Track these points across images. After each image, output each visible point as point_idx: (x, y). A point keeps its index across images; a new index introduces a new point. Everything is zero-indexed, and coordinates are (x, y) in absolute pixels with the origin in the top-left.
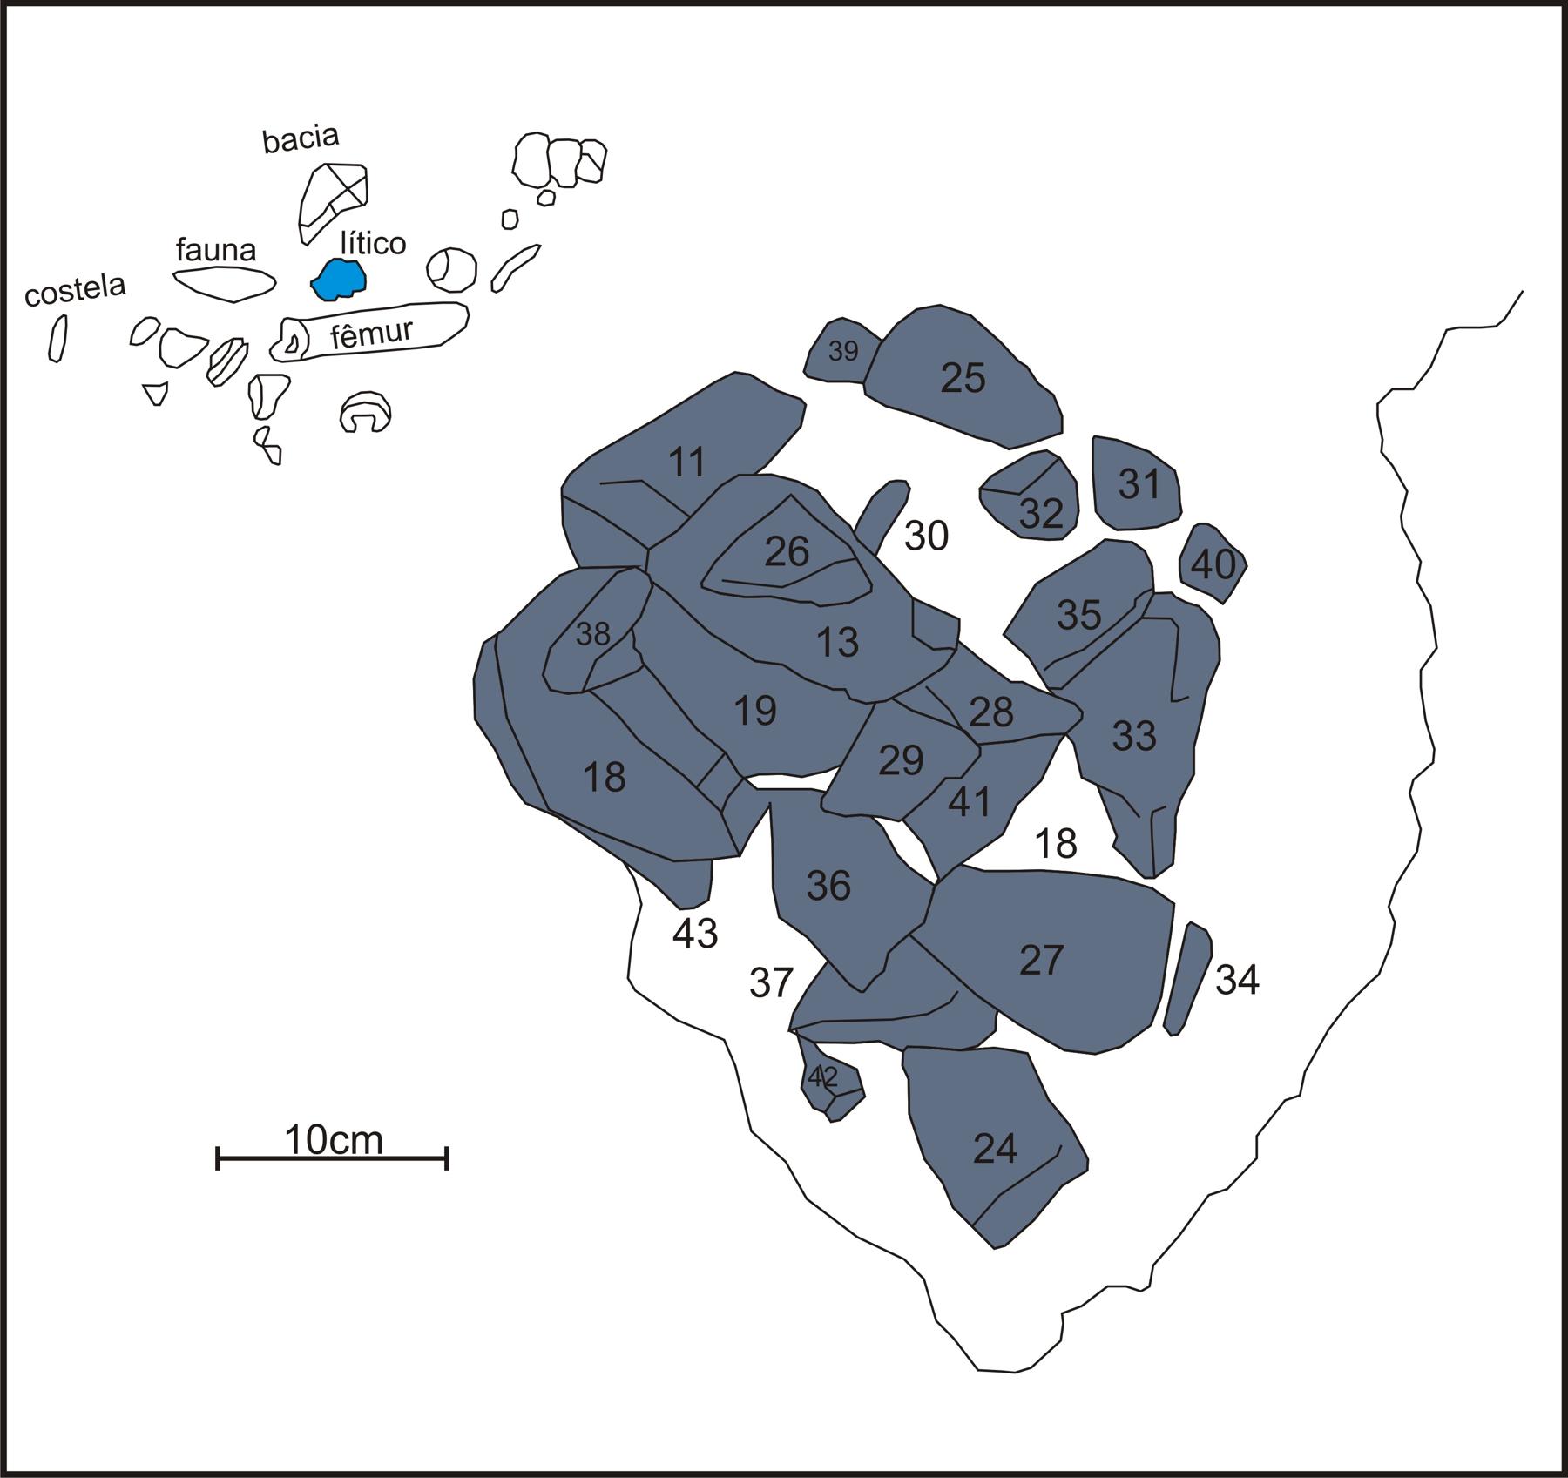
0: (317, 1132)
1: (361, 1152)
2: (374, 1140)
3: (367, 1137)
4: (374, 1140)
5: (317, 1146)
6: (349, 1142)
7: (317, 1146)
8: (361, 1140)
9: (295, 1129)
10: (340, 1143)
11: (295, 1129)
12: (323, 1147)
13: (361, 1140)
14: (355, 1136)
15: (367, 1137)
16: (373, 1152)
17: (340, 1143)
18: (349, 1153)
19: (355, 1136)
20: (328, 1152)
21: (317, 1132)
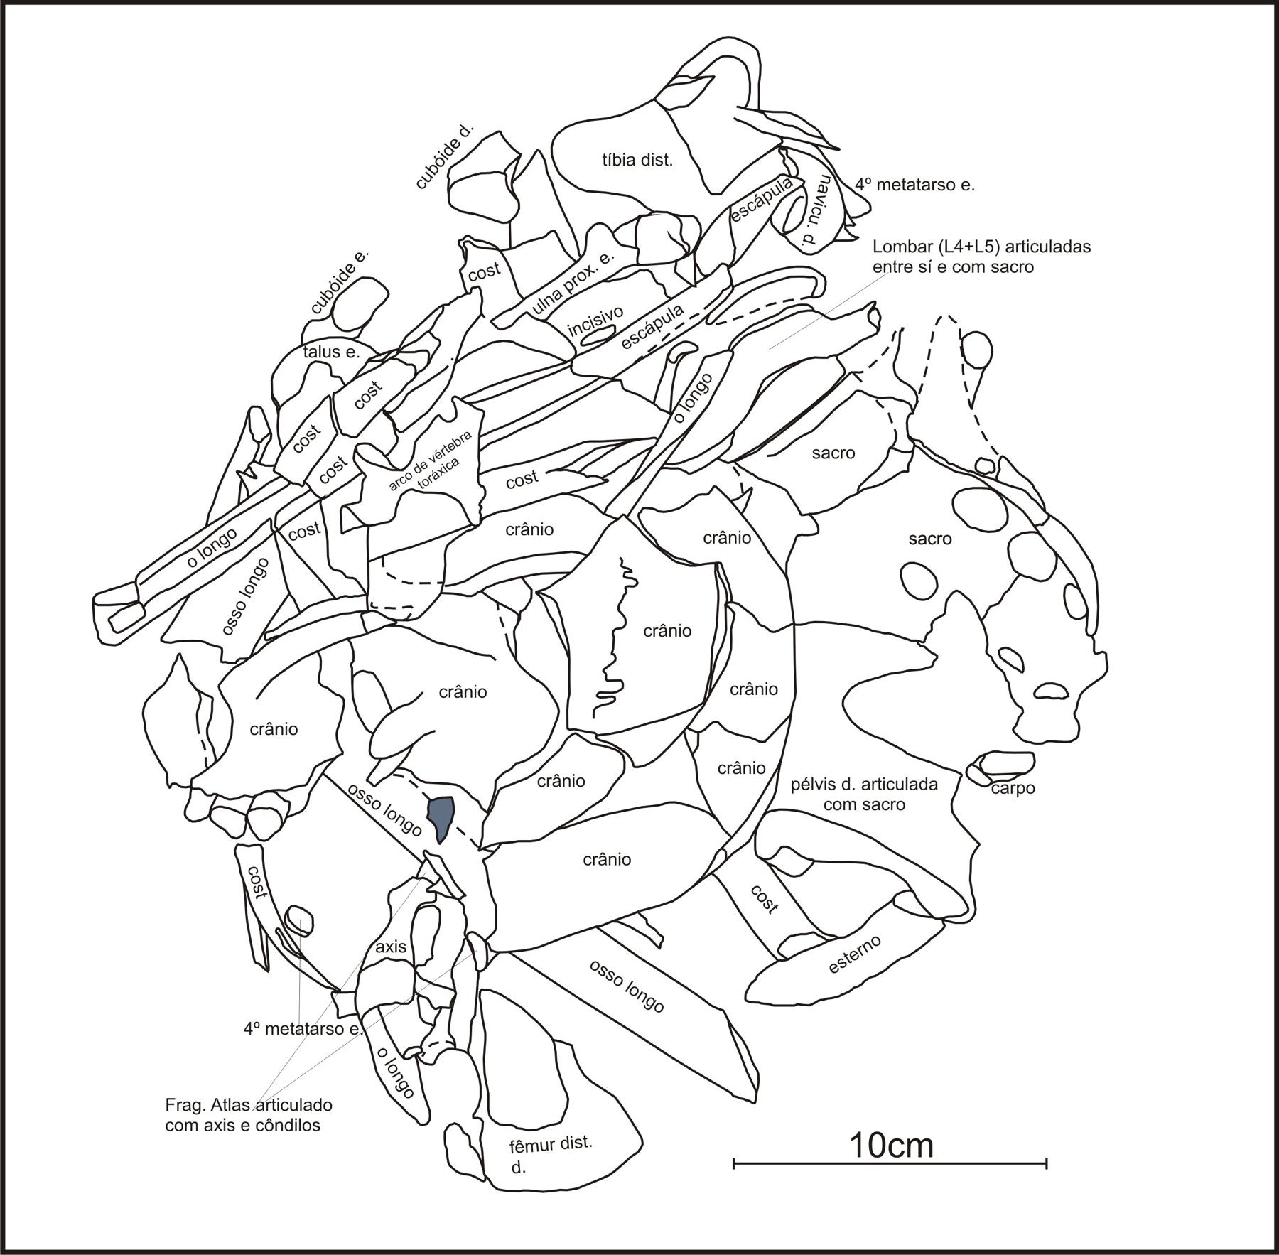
0: (877, 1139)
2: (925, 1145)
3: (920, 1143)
4: (925, 1145)
5: (877, 1151)
6: (905, 1148)
7: (877, 1151)
8: (915, 1145)
9: (858, 1136)
10: (897, 1148)
11: (858, 1136)
13: (915, 1145)
14: (909, 1142)
15: (920, 1143)
17: (897, 1148)
18: (904, 1159)
19: (909, 1142)
21: (877, 1139)
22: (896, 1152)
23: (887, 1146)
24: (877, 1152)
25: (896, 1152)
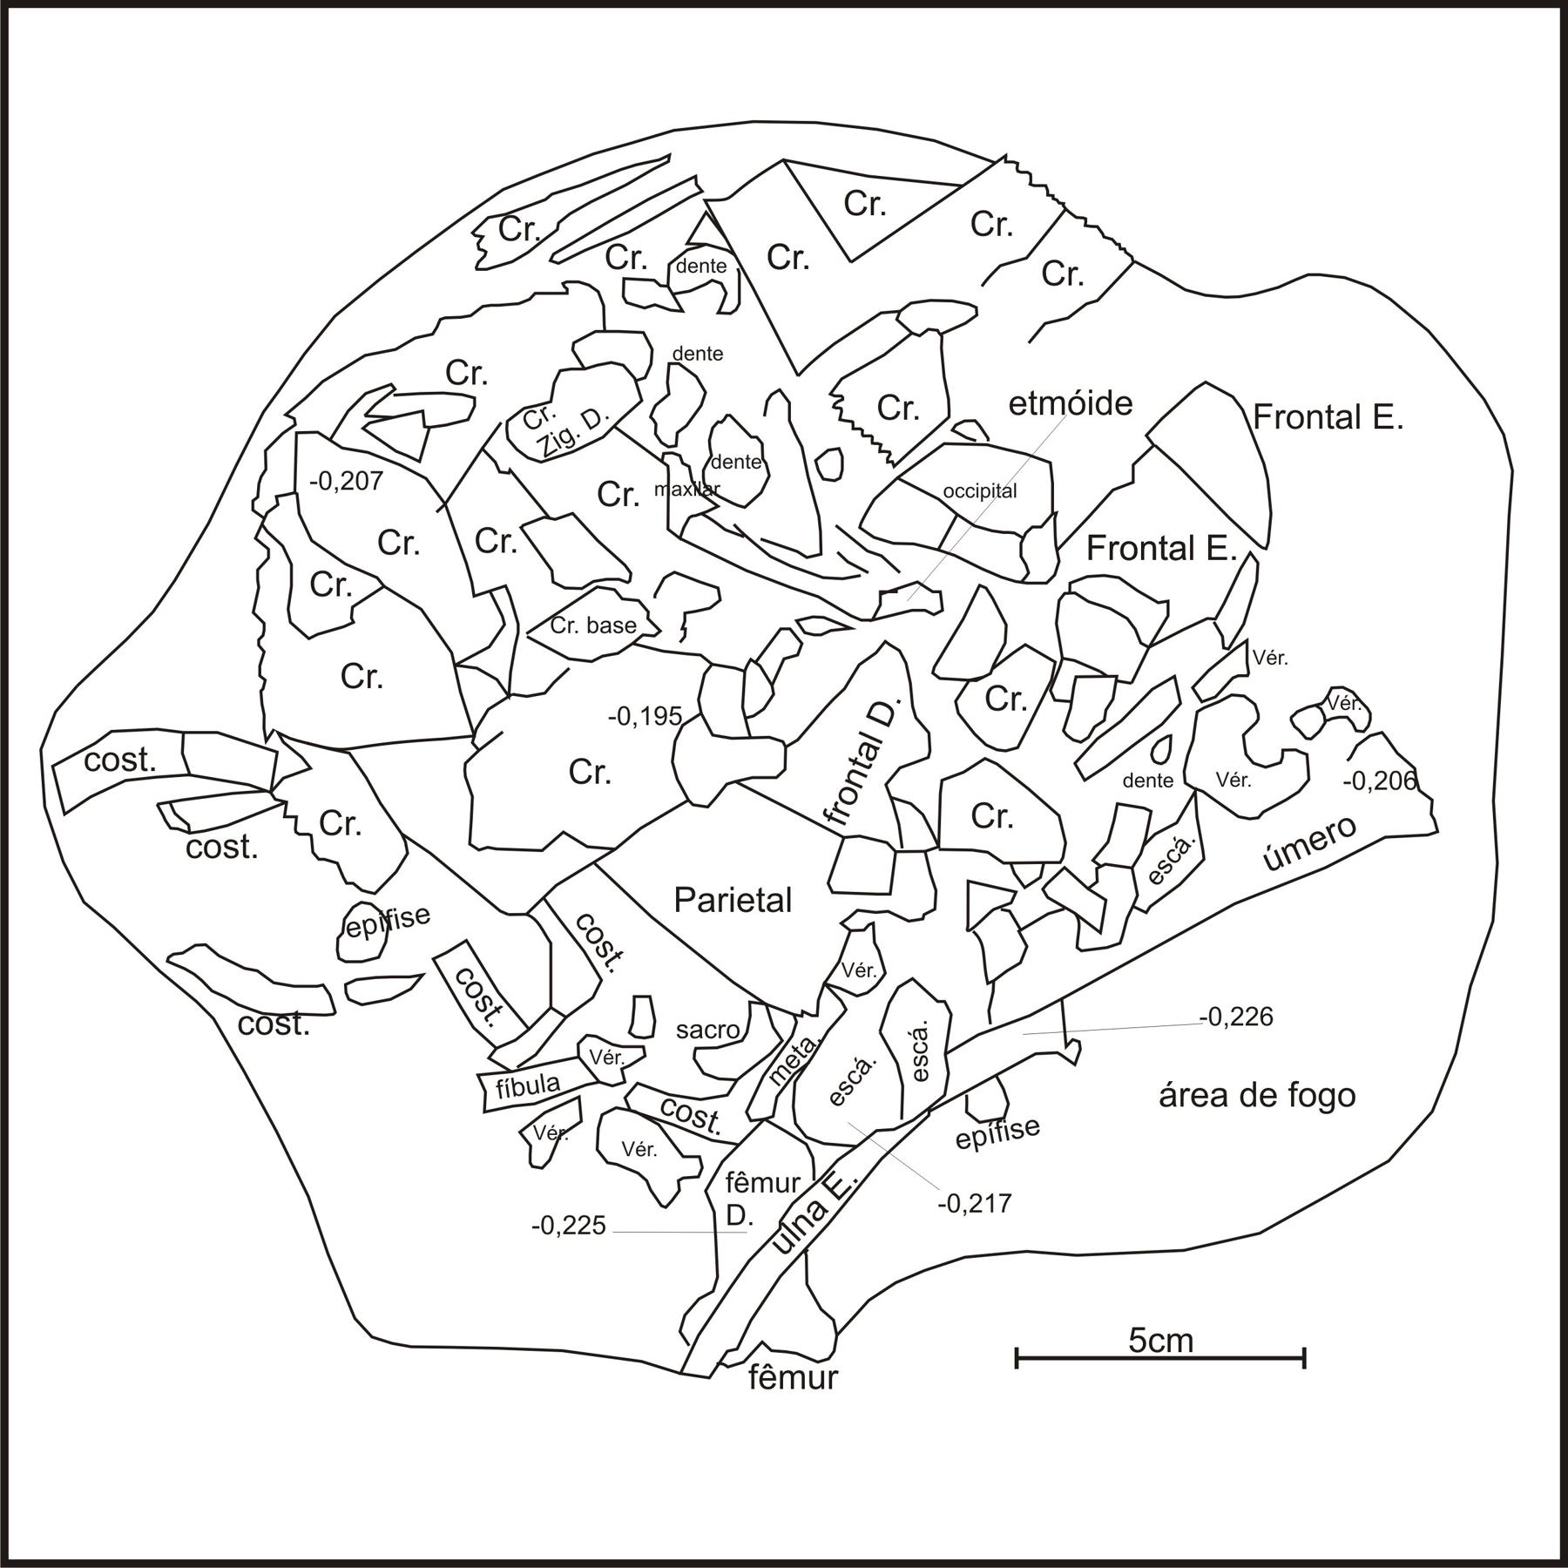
1: (1175, 1352)
2: (1186, 1340)
3: (1180, 1338)
4: (1186, 1340)
6: (1165, 1342)
8: (1175, 1340)
10: (1157, 1343)
12: (1147, 1348)
13: (1175, 1340)
14: (1170, 1337)
15: (1180, 1338)
16: (1185, 1352)
17: (1157, 1343)
18: (1165, 1353)
19: (1170, 1337)
20: (1148, 1352)
22: (1157, 1347)
25: (1157, 1347)
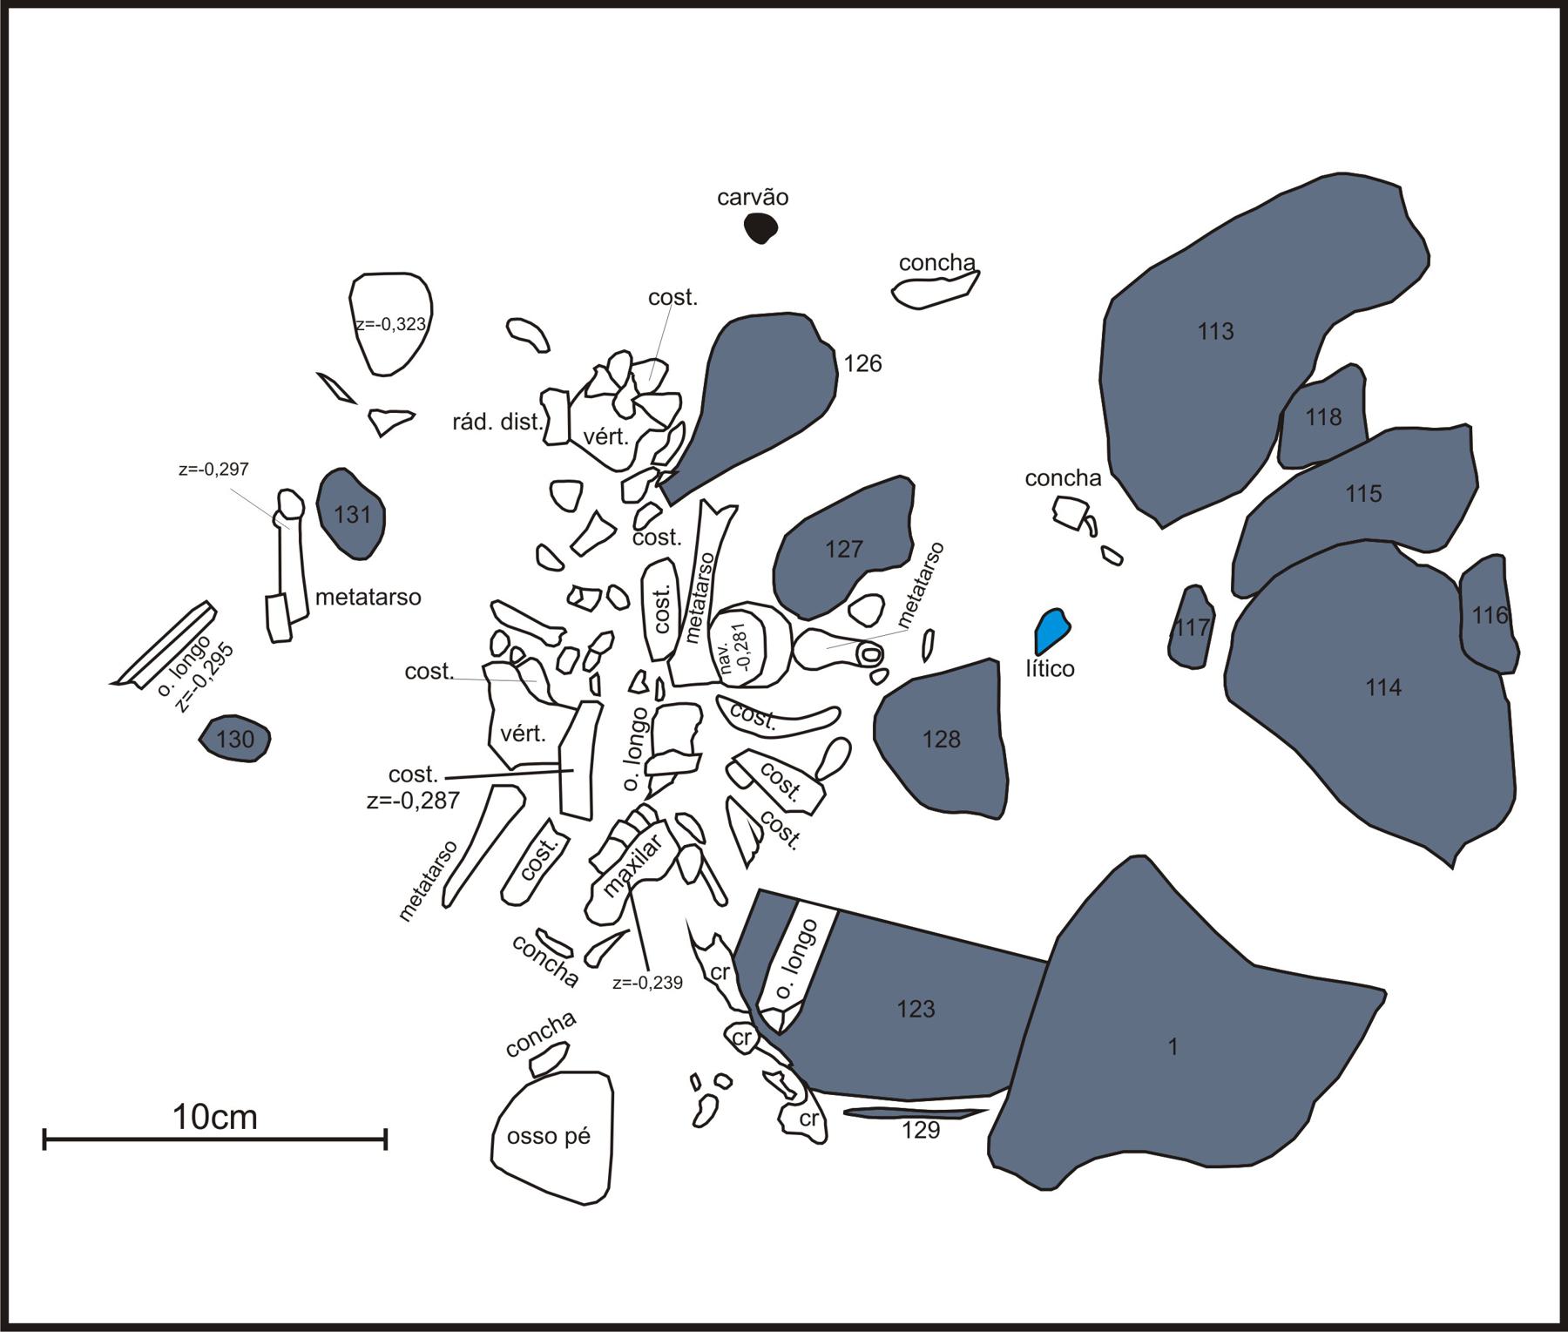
0: (200, 1110)
2: (249, 1117)
3: (244, 1115)
4: (249, 1117)
5: (200, 1121)
7: (200, 1121)
8: (238, 1117)
9: (182, 1107)
11: (182, 1107)
13: (238, 1117)
14: (233, 1114)
15: (244, 1115)
19: (233, 1114)
21: (200, 1110)
22: (220, 1124)
23: (210, 1118)
24: (200, 1124)
25: (220, 1124)
